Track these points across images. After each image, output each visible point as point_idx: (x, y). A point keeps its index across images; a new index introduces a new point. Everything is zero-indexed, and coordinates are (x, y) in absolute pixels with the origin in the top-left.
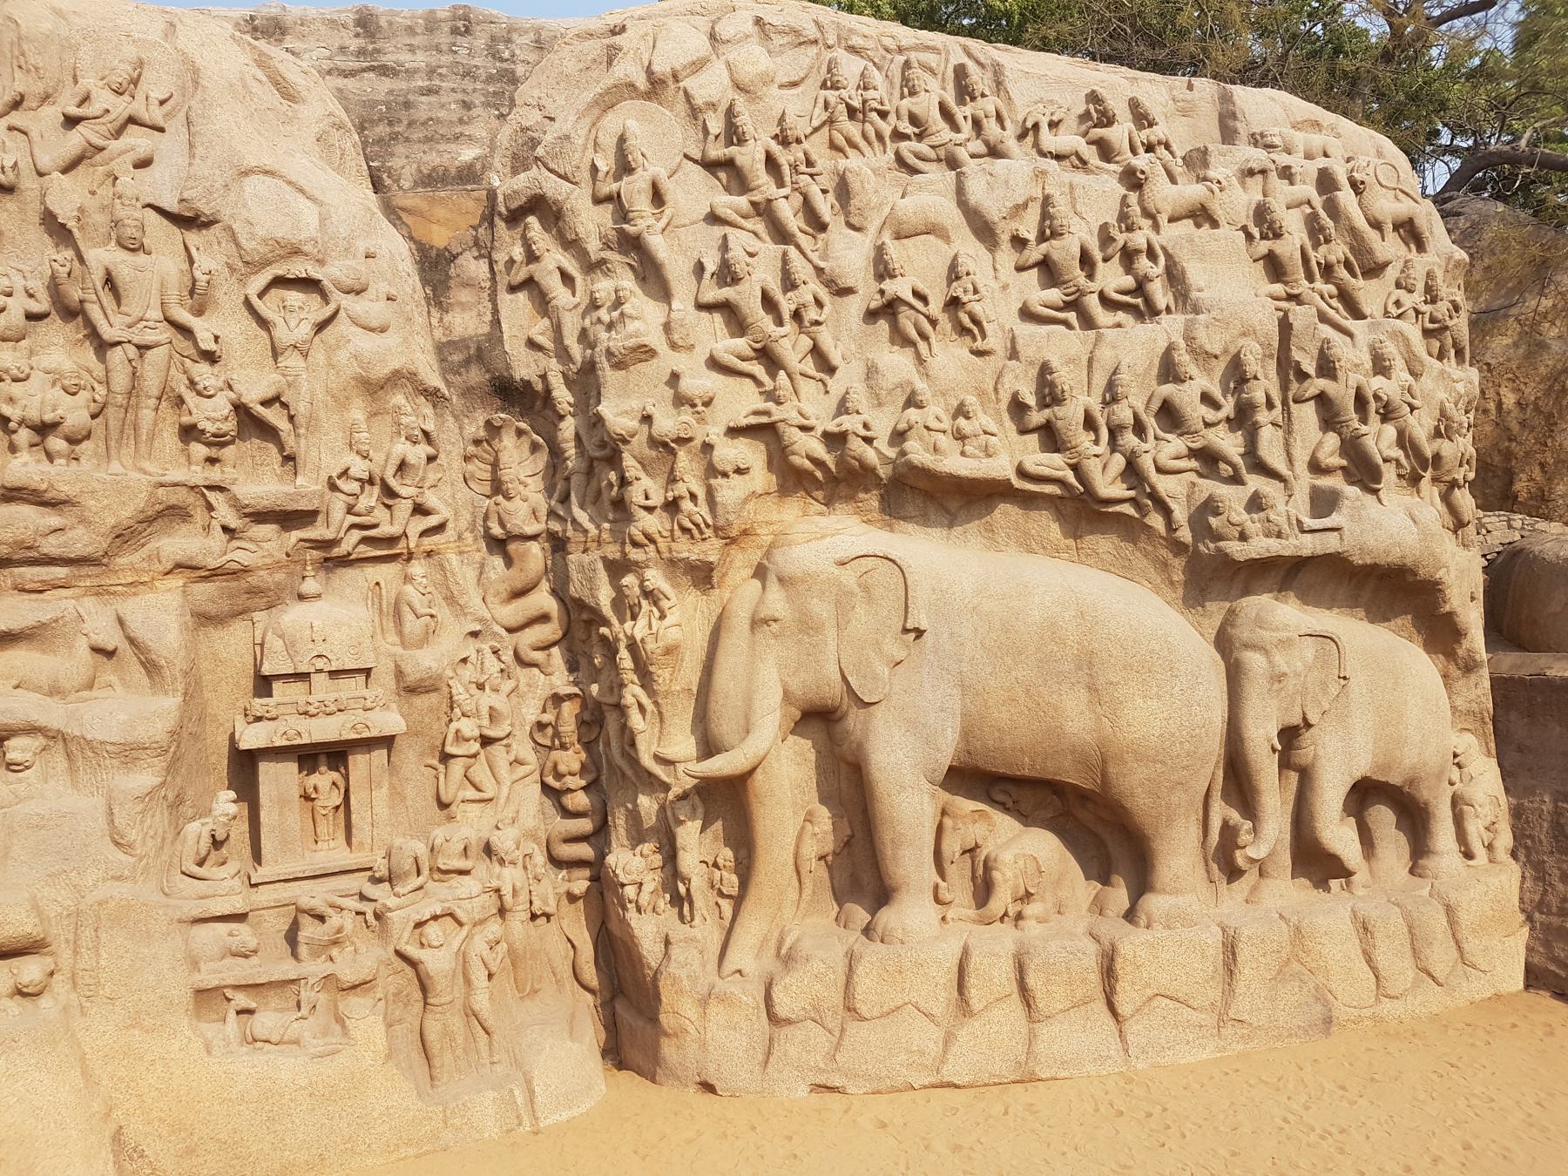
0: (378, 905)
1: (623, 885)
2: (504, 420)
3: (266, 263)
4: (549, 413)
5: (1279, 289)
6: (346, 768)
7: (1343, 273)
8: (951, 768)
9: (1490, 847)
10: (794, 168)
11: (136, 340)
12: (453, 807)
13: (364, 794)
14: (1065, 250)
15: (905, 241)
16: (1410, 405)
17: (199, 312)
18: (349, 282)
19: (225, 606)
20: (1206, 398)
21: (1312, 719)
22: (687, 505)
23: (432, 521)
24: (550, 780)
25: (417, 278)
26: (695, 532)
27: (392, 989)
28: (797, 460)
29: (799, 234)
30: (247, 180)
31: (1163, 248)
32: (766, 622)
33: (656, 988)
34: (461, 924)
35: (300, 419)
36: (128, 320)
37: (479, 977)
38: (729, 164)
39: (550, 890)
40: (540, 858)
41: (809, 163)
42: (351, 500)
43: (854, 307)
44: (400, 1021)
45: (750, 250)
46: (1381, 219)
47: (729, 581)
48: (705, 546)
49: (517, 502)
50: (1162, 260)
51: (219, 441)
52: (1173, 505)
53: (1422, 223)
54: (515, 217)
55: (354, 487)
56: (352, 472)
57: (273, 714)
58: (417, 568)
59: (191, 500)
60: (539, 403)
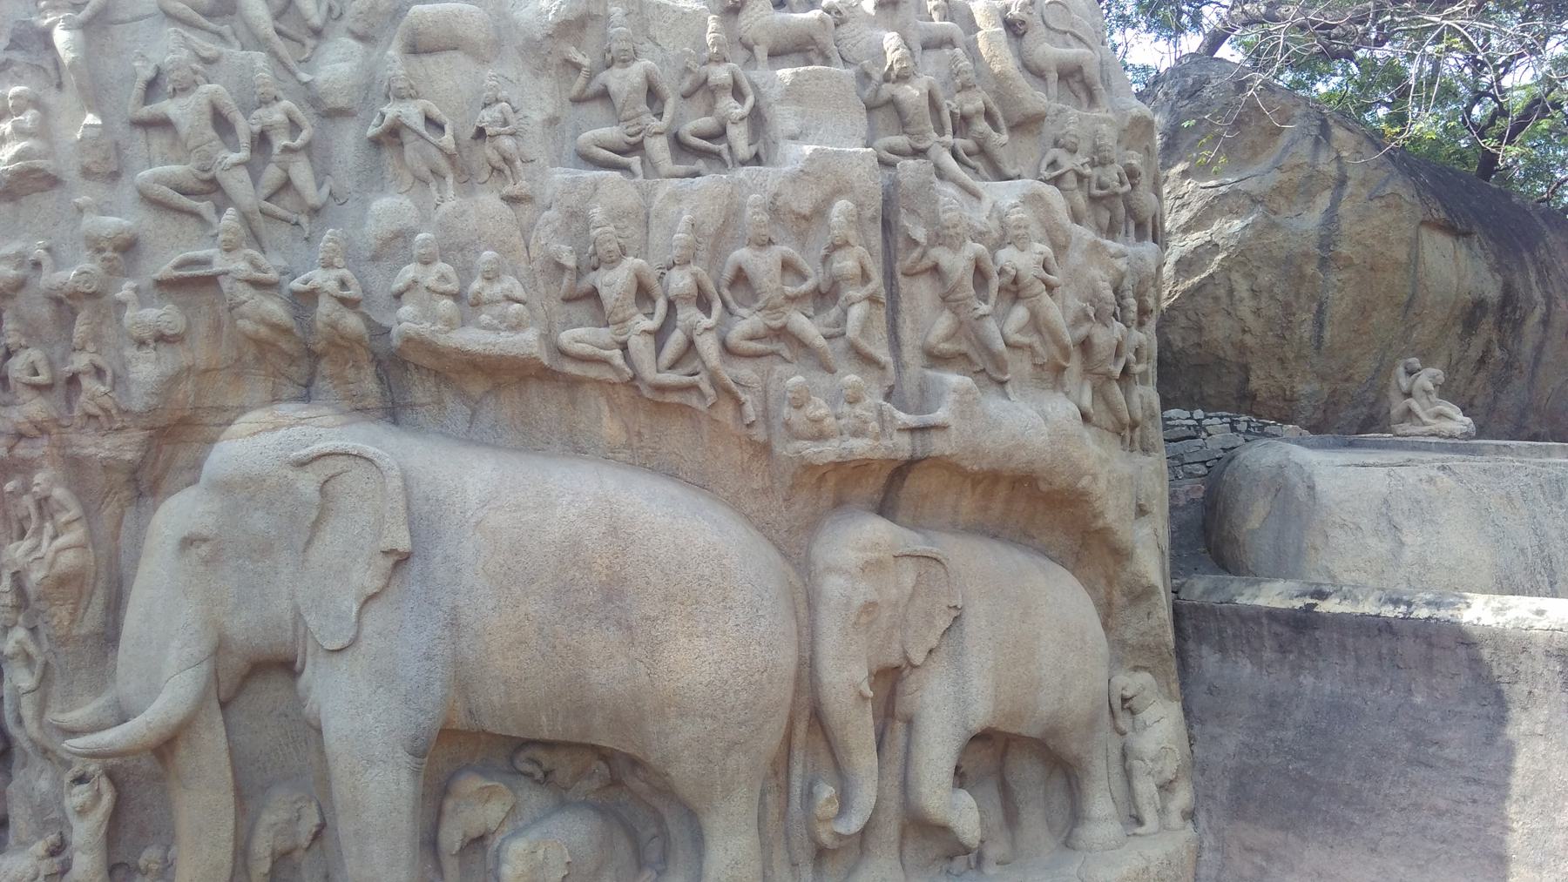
5: (901, 141)
7: (982, 126)
8: (442, 731)
9: (1162, 812)
14: (624, 80)
15: (429, 60)
16: (1044, 282)
20: (787, 266)
21: (918, 657)
22: (88, 383)
26: (102, 419)
28: (247, 325)
29: (276, 38)
31: (754, 86)
32: (188, 542)
43: (348, 141)
45: (206, 54)
46: (1043, 65)
48: (118, 440)
50: (750, 101)
52: (744, 397)
53: (1092, 71)
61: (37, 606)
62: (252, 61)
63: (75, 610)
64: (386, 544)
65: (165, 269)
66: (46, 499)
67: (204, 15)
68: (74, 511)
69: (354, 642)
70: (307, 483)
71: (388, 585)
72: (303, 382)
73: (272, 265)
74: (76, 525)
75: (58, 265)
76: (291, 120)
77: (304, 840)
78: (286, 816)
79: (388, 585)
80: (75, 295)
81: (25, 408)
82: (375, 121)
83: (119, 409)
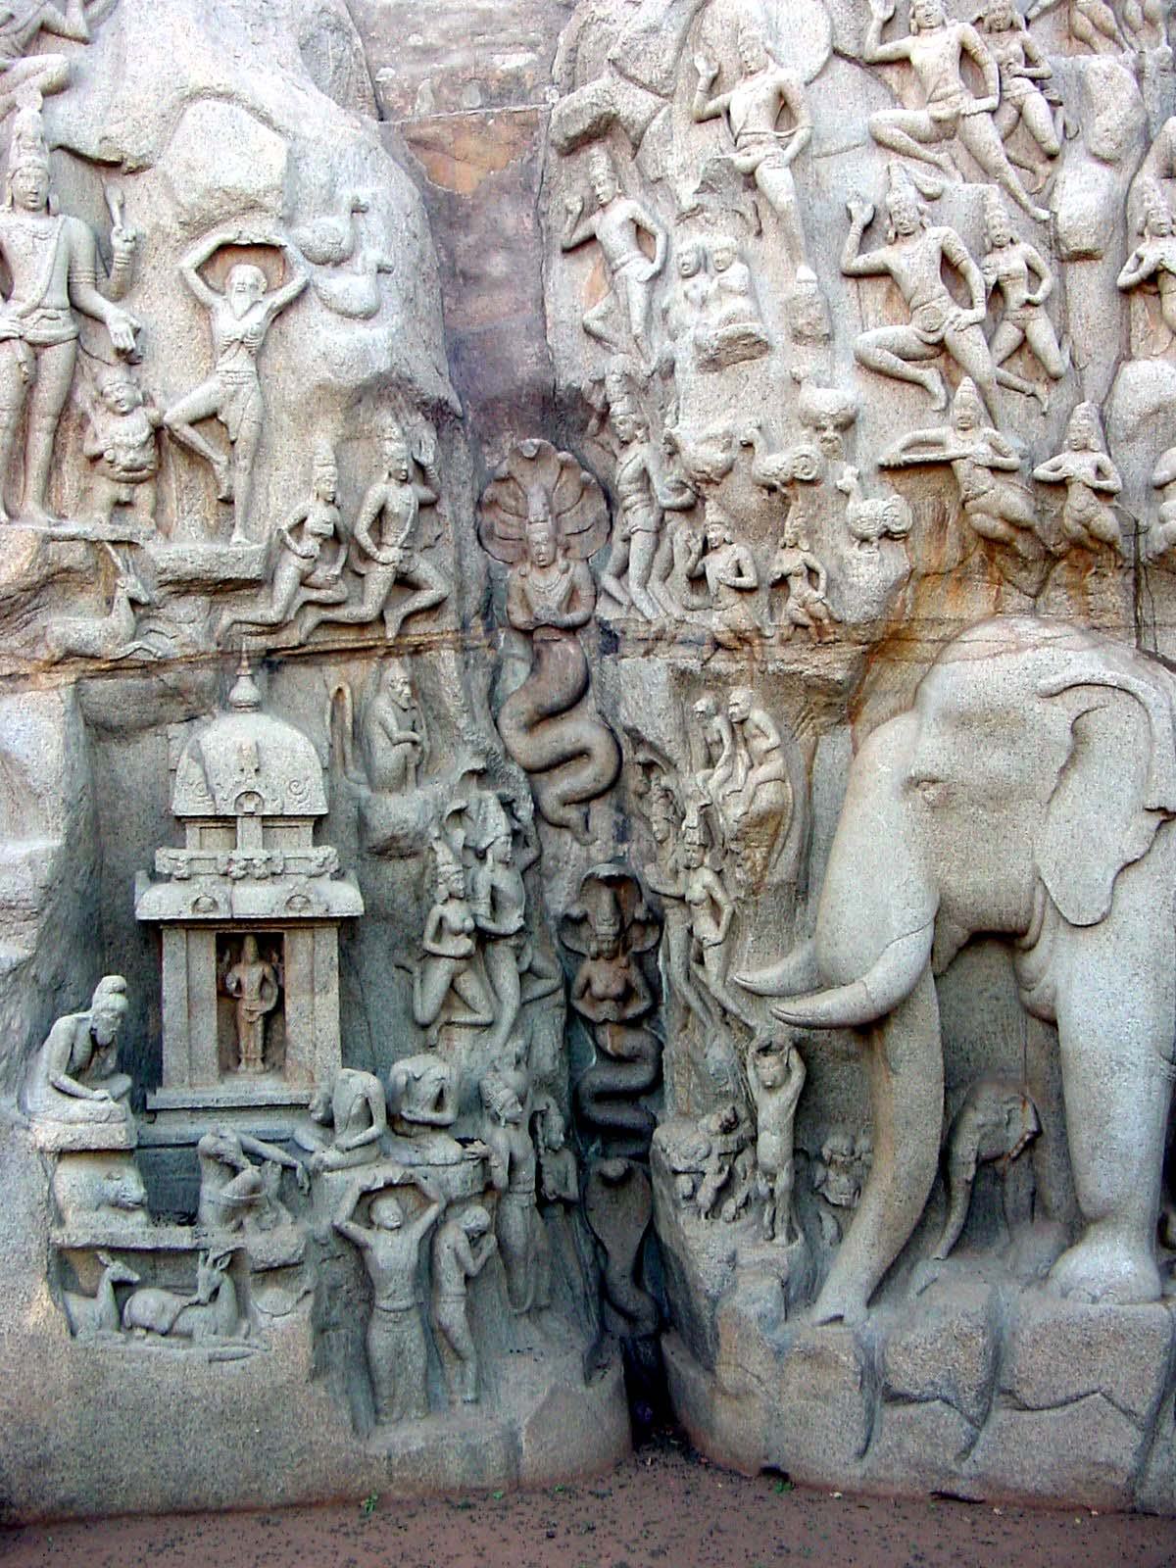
0: (312, 1160)
1: (676, 1173)
2: (539, 448)
3: (207, 224)
4: (605, 437)
6: (281, 959)
10: (1002, 65)
11: (30, 336)
12: (433, 1032)
13: (305, 999)
17: (118, 296)
18: (326, 248)
19: (131, 713)
22: (798, 585)
23: (423, 599)
24: (581, 1006)
25: (429, 239)
26: (812, 630)
27: (327, 1281)
29: (1009, 168)
30: (193, 109)
32: (915, 783)
33: (714, 1326)
34: (426, 1201)
35: (240, 446)
36: (21, 307)
37: (451, 1283)
38: (904, 61)
39: (572, 1166)
40: (556, 1121)
41: (1029, 61)
42: (305, 564)
44: (336, 1325)
45: (928, 190)
47: (867, 712)
49: (554, 573)
51: (134, 477)
54: (575, 146)
55: (310, 545)
56: (308, 524)
57: (184, 872)
58: (397, 672)
59: (91, 561)
60: (594, 422)
61: (733, 846)
62: (983, 196)
63: (769, 853)
64: (1153, 802)
65: (892, 454)
66: (742, 722)
67: (920, 142)
68: (774, 739)
69: (1105, 917)
70: (1057, 717)
71: (1149, 851)
72: (1032, 591)
73: (1013, 447)
74: (775, 754)
75: (771, 448)
76: (1029, 267)
77: (1013, 1147)
78: (995, 1118)
79: (1149, 851)
80: (793, 482)
81: (727, 614)
82: (1130, 264)
83: (831, 618)
